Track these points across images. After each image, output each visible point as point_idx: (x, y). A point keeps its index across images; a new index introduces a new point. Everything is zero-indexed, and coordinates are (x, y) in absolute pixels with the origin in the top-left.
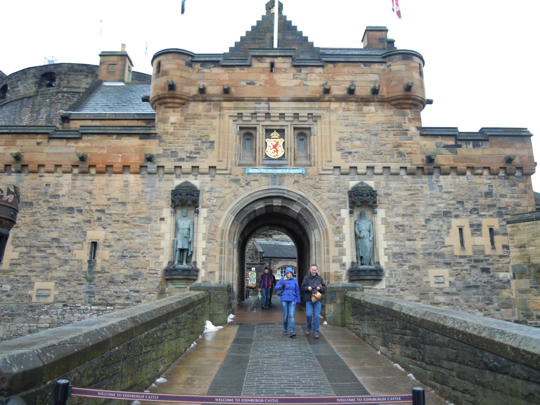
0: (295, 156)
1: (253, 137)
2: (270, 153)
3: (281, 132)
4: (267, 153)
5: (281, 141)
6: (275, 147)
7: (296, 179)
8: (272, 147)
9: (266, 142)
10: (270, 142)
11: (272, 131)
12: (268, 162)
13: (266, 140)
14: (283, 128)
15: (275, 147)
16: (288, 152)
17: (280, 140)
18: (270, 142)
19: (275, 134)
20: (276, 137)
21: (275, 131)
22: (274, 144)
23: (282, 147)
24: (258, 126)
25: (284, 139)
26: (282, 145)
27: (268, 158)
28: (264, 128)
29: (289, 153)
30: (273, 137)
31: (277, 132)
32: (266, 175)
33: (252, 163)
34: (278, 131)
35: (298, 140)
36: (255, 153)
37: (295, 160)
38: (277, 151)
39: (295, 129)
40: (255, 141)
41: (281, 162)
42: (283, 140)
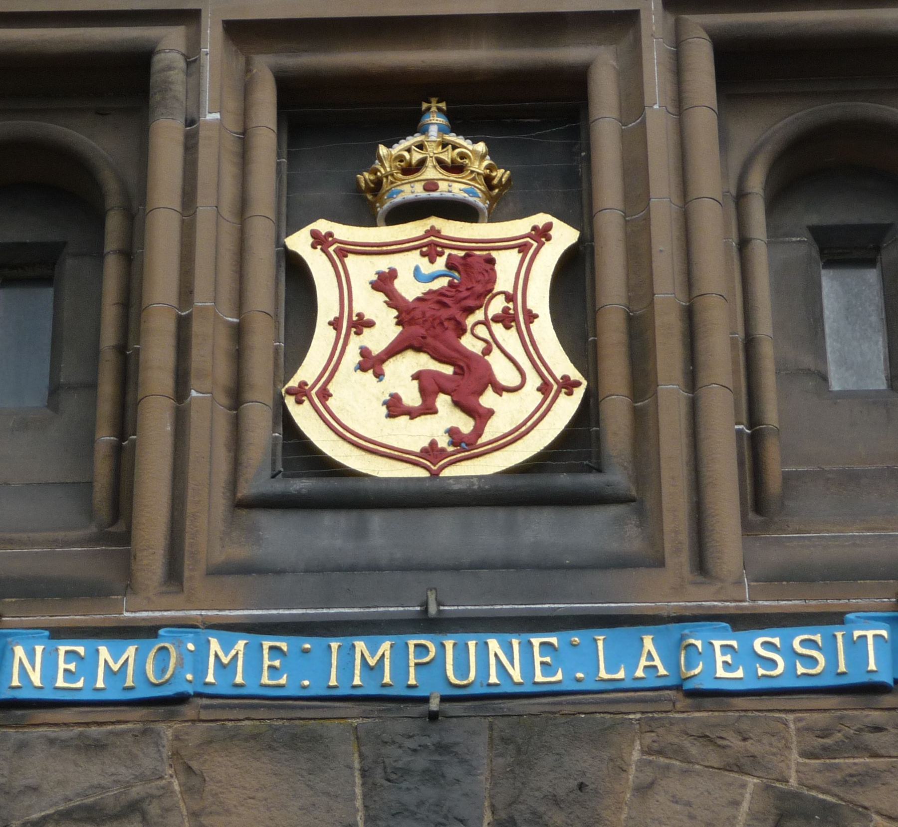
0: (753, 445)
1: (96, 217)
2: (363, 410)
3: (535, 122)
4: (304, 417)
5: (528, 256)
6: (430, 325)
7: (795, 770)
8: (385, 330)
9: (296, 272)
10: (362, 270)
11: (391, 107)
12: (329, 534)
13: (299, 242)
14: (569, 53)
15: (430, 325)
16: (641, 382)
17: (521, 227)
18: (362, 270)
19: (435, 154)
20: (454, 188)
21: (435, 121)
22: (409, 289)
23: (544, 331)
24: (171, 41)
25: (578, 209)
26: (539, 297)
27: (311, 482)
28: (265, 66)
29: (670, 389)
30: (411, 190)
31: (460, 123)
32: (286, 725)
33: (76, 560)
34: (476, 106)
35: (801, 247)
36: (125, 423)
37: (758, 501)
38: (468, 383)
39: (745, 69)
40: (132, 256)
41: (539, 530)
42: (565, 236)
